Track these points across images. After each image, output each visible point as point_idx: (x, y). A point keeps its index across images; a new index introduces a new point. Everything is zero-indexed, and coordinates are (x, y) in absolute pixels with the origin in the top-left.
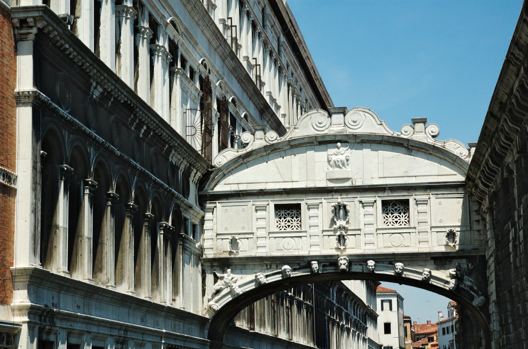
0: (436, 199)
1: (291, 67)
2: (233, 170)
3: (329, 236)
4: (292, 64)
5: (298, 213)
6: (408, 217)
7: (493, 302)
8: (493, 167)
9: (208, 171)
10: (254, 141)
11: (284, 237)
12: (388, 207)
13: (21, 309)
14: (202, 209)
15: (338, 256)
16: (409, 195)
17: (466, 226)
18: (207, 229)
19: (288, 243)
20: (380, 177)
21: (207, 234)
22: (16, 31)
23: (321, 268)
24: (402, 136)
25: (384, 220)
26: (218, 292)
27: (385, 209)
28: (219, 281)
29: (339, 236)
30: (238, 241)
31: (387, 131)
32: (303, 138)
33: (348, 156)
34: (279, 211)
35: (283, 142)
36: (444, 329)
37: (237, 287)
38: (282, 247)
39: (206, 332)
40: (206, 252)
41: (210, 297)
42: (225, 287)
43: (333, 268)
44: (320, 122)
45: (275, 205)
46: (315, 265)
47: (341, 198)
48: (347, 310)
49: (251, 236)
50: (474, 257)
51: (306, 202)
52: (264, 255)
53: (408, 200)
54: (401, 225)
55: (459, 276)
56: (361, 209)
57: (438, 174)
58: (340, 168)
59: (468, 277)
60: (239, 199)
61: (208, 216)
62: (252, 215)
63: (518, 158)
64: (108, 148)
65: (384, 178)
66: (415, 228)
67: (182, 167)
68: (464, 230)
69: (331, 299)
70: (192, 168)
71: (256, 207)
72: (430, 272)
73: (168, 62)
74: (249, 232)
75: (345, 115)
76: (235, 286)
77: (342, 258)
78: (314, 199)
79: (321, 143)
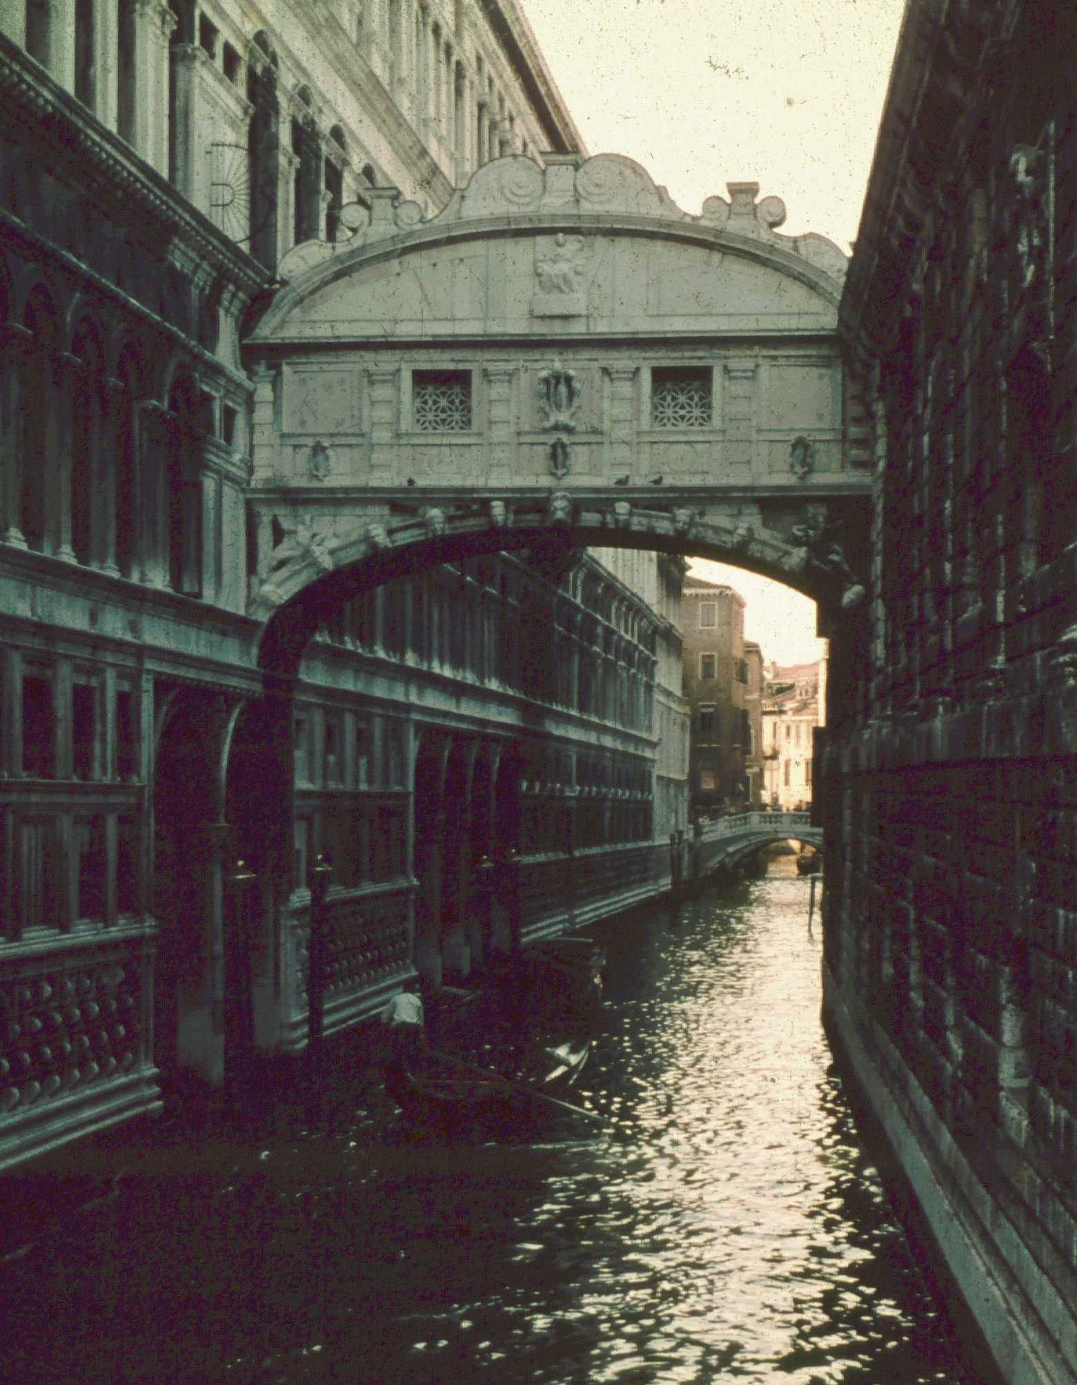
1: (487, 67)
3: (532, 444)
4: (489, 56)
9: (263, 291)
10: (370, 224)
14: (250, 378)
15: (550, 490)
16: (714, 358)
23: (511, 517)
26: (282, 564)
28: (285, 540)
29: (554, 446)
30: (330, 452)
39: (255, 651)
43: (537, 517)
48: (608, 619)
49: (360, 440)
54: (692, 425)
56: (608, 388)
58: (561, 291)
61: (264, 392)
62: (360, 391)
63: (929, 268)
67: (200, 279)
69: (569, 595)
73: (168, 32)
77: (559, 494)
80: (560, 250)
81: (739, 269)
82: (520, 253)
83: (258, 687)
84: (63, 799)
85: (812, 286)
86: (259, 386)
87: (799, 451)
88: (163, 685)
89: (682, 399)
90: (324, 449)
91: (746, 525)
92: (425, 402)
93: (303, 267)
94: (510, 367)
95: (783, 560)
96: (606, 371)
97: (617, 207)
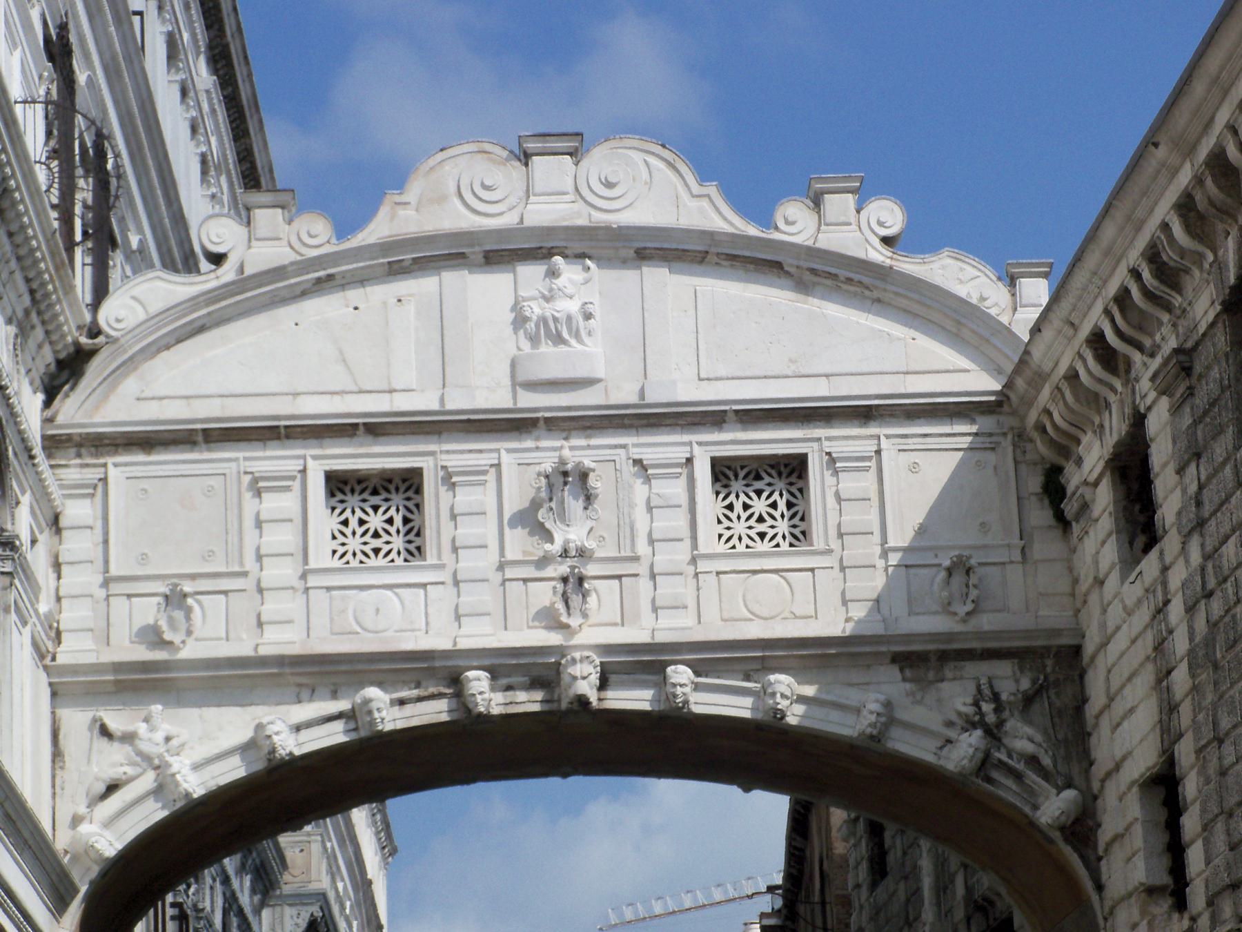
0: (901, 453)
2: (168, 347)
3: (525, 581)
5: (410, 504)
6: (802, 519)
7: (1133, 783)
8: (1183, 252)
9: (76, 344)
10: (250, 247)
11: (362, 588)
12: (733, 483)
15: (561, 651)
17: (1008, 546)
18: (72, 559)
19: (378, 610)
20: (702, 376)
21: (73, 579)
23: (499, 697)
24: (777, 236)
25: (720, 529)
27: (720, 489)
29: (565, 580)
30: (190, 601)
31: (725, 219)
32: (431, 239)
33: (591, 303)
34: (340, 496)
35: (357, 253)
37: (186, 770)
38: (351, 619)
41: (82, 810)
42: (139, 770)
44: (487, 183)
46: (478, 683)
47: (572, 448)
50: (1042, 652)
51: (444, 464)
54: (778, 545)
55: (991, 718)
56: (640, 491)
57: (904, 369)
59: (1019, 725)
60: (192, 451)
61: (76, 511)
65: (717, 379)
66: (830, 552)
68: (1002, 560)
70: (34, 315)
71: (256, 480)
74: (230, 570)
75: (576, 165)
78: (470, 451)
80: (560, 282)
86: (69, 503)
87: (958, 579)
89: (760, 506)
90: (185, 596)
91: (882, 698)
92: (345, 523)
93: (142, 316)
94: (485, 460)
95: (946, 749)
96: (638, 462)
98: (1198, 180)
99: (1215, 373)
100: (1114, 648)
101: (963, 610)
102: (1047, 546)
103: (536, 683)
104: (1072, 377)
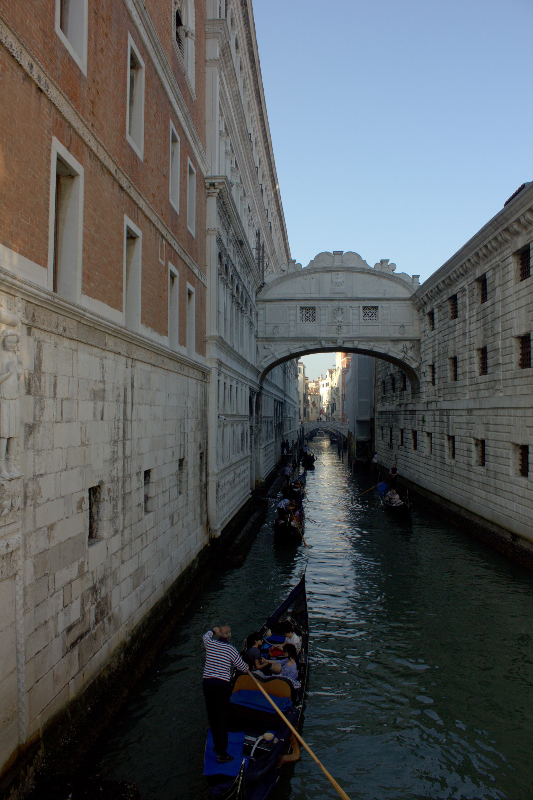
13: (211, 360)
15: (337, 338)
21: (261, 323)
22: (207, 191)
36: (323, 385)
39: (259, 380)
40: (259, 333)
43: (334, 344)
45: (300, 307)
46: (323, 342)
49: (286, 325)
50: (414, 340)
52: (294, 336)
53: (378, 307)
61: (261, 312)
64: (234, 267)
72: (389, 348)
76: (276, 354)
79: (327, 272)
80: (339, 276)
81: (385, 282)
82: (327, 277)
83: (258, 389)
84: (240, 419)
85: (404, 286)
87: (402, 328)
88: (250, 389)
89: (370, 314)
94: (326, 306)
97: (353, 264)
98: (446, 279)
99: (446, 308)
100: (426, 343)
101: (402, 333)
102: (417, 323)
103: (333, 343)
104: (422, 299)
